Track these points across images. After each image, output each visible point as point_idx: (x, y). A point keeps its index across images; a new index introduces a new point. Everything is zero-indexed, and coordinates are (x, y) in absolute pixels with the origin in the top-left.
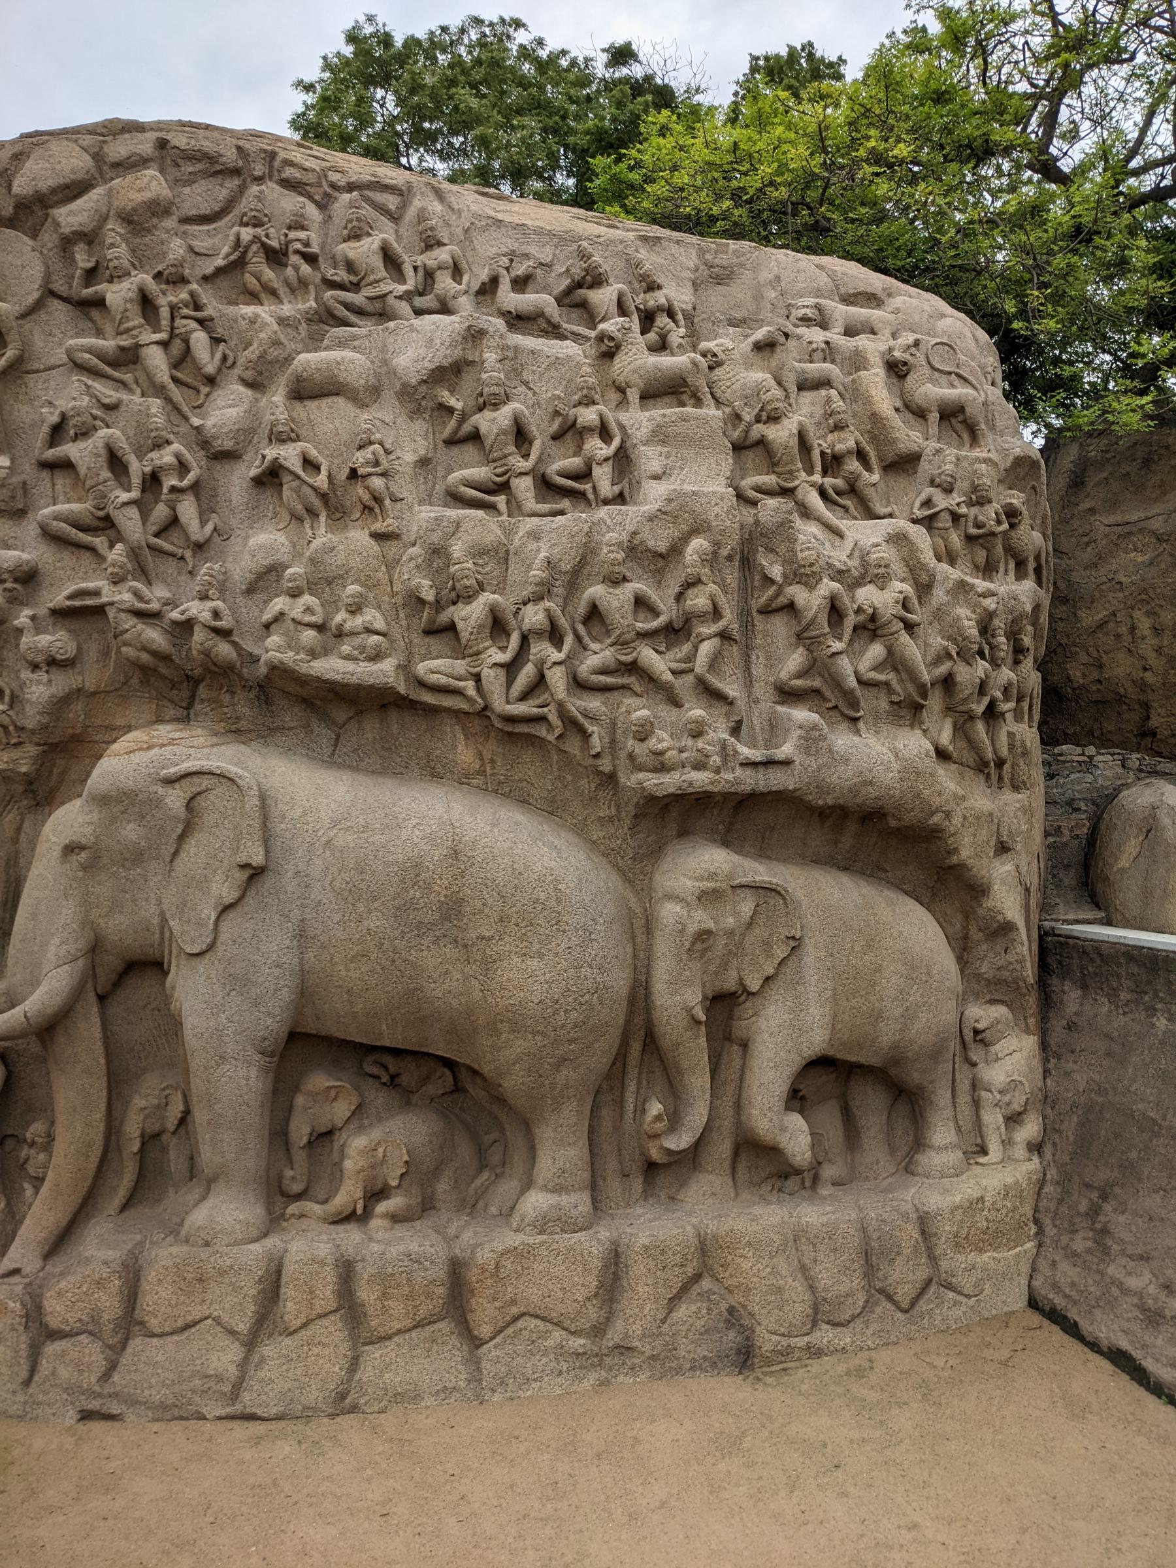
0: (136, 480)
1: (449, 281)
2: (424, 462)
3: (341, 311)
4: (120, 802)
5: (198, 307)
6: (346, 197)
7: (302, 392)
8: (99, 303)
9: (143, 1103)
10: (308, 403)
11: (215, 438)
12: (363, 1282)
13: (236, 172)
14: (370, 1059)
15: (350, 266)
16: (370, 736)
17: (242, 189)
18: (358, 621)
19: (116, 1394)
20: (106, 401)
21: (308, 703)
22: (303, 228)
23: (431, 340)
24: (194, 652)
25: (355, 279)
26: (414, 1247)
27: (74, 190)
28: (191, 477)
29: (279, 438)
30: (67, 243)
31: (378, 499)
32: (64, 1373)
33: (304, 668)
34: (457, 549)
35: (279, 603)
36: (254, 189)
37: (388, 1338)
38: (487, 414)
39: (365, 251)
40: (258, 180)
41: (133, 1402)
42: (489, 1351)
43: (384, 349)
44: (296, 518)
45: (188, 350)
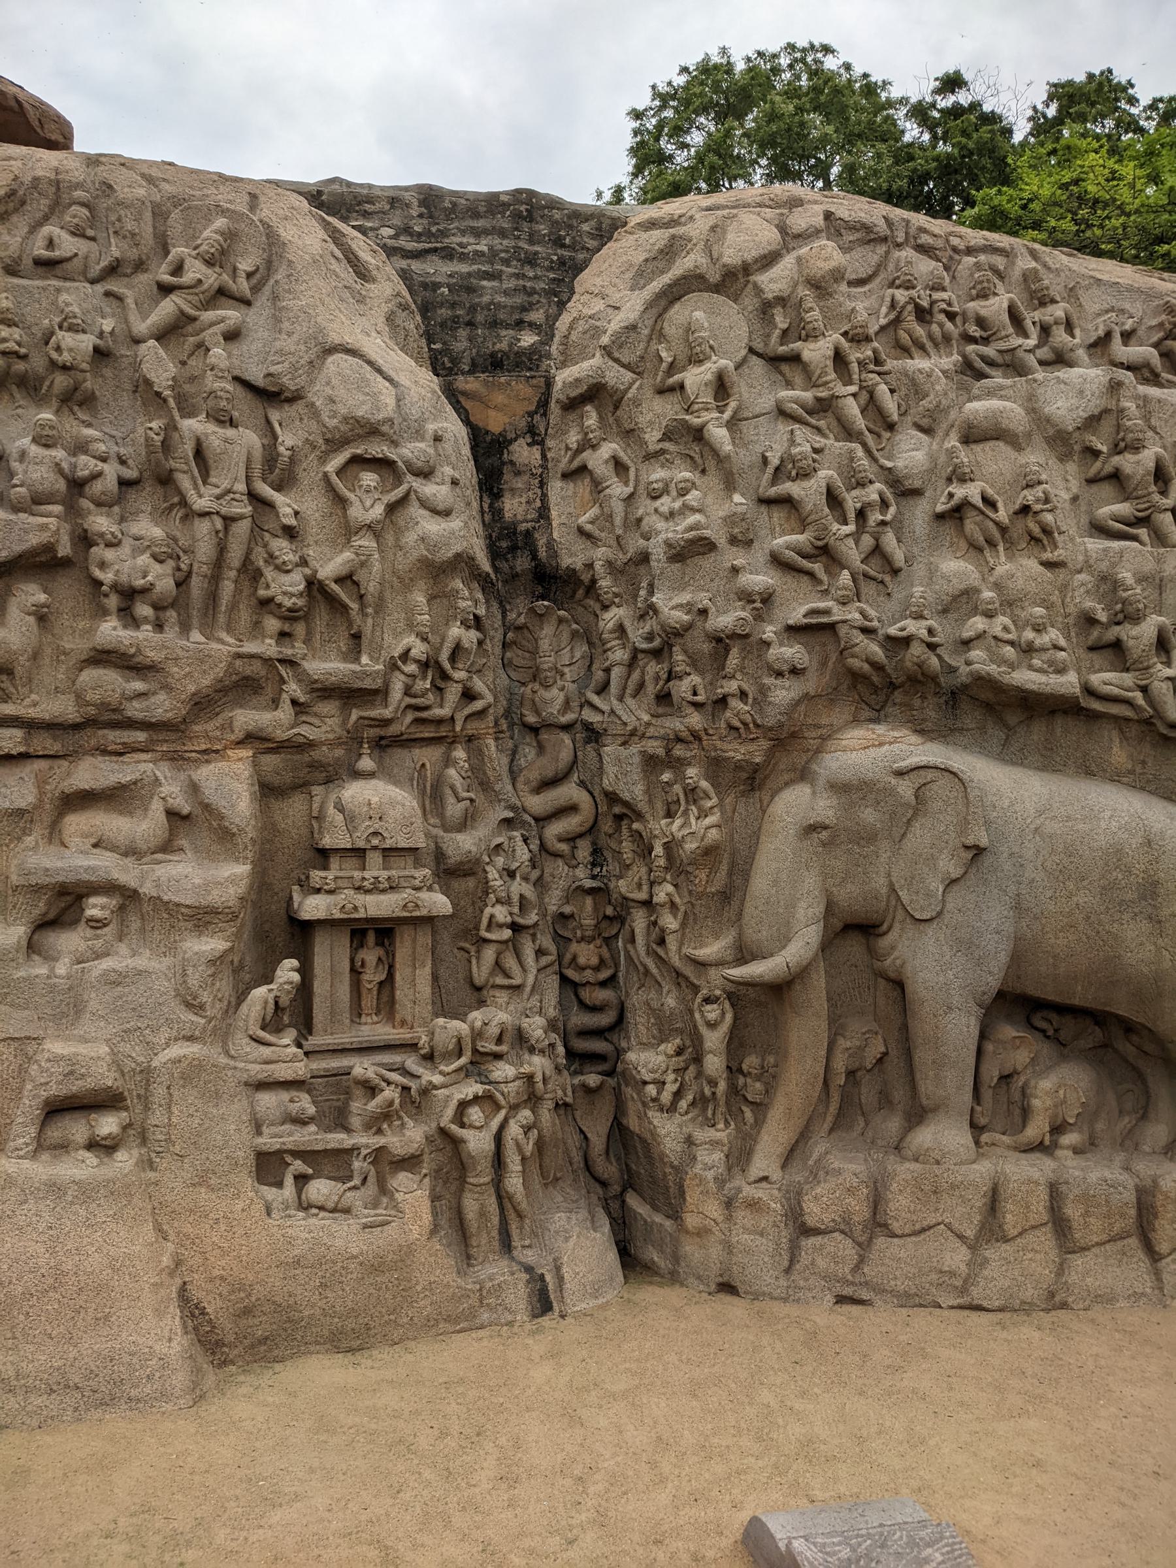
0: (851, 515)
1: (1065, 335)
2: (1075, 499)
3: (979, 364)
4: (848, 790)
5: (878, 361)
6: (970, 260)
7: (972, 436)
8: (795, 359)
9: (849, 1044)
10: (973, 446)
11: (906, 477)
12: (1068, 1202)
13: (885, 239)
14: (1039, 1015)
15: (981, 322)
16: (1035, 738)
17: (887, 253)
18: (1044, 639)
19: (866, 1283)
20: (817, 446)
21: (988, 707)
22: (944, 289)
23: (1081, 392)
24: (908, 664)
25: (985, 335)
26: (1107, 1174)
27: (769, 260)
28: (892, 510)
29: (959, 476)
30: (766, 308)
31: (1047, 531)
32: (822, 1263)
33: (1006, 679)
34: (1126, 575)
35: (978, 623)
36: (897, 254)
37: (1084, 1249)
38: (1128, 456)
39: (995, 307)
40: (898, 245)
41: (880, 1290)
42: (1168, 1265)
43: (1031, 397)
44: (975, 547)
45: (871, 397)
